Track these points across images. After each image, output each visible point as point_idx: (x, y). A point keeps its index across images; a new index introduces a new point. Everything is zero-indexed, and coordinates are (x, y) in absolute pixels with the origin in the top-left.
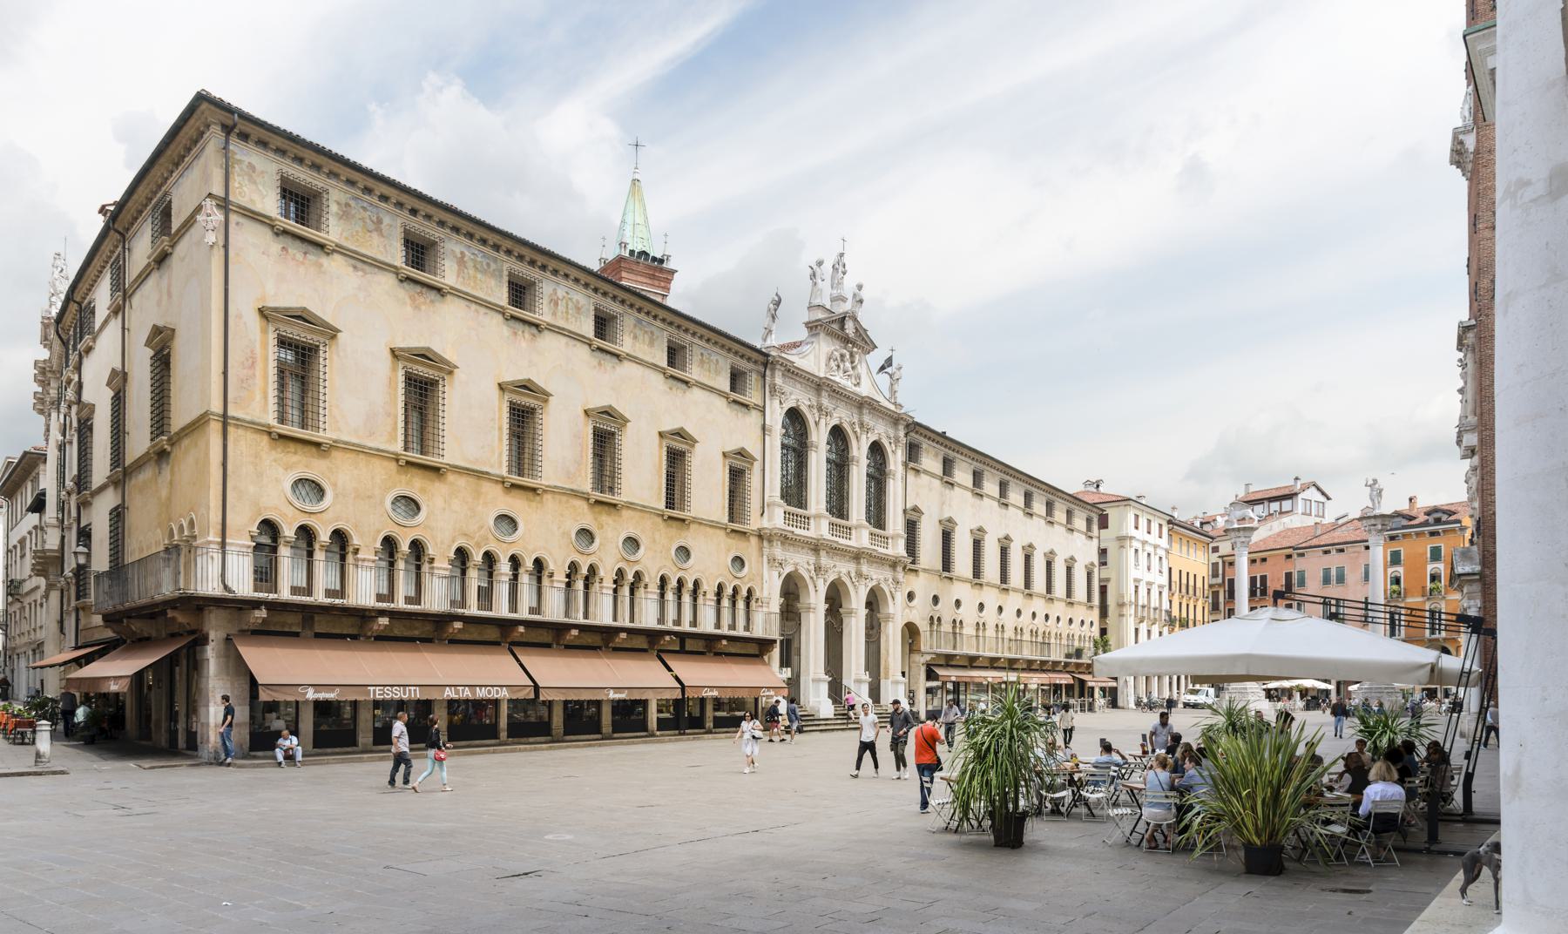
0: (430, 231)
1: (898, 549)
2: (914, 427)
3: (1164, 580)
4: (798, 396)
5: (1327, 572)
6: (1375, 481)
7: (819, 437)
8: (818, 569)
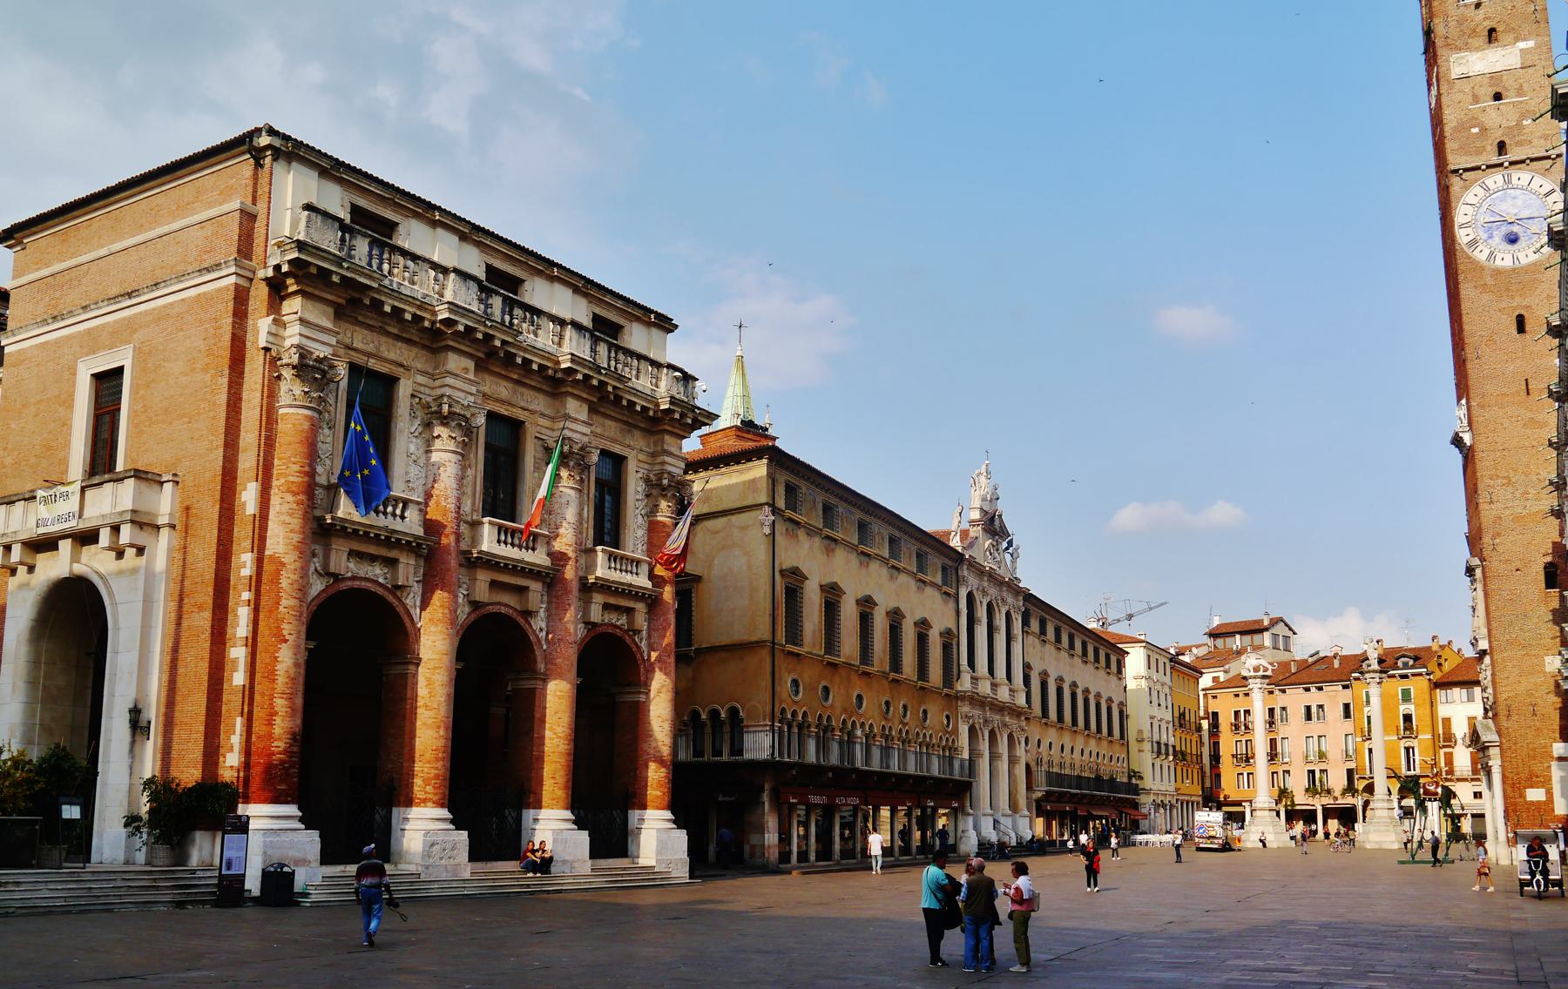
0: (833, 501)
1: (1021, 700)
2: (1030, 598)
4: (972, 581)
5: (1308, 708)
7: (982, 613)
8: (986, 721)
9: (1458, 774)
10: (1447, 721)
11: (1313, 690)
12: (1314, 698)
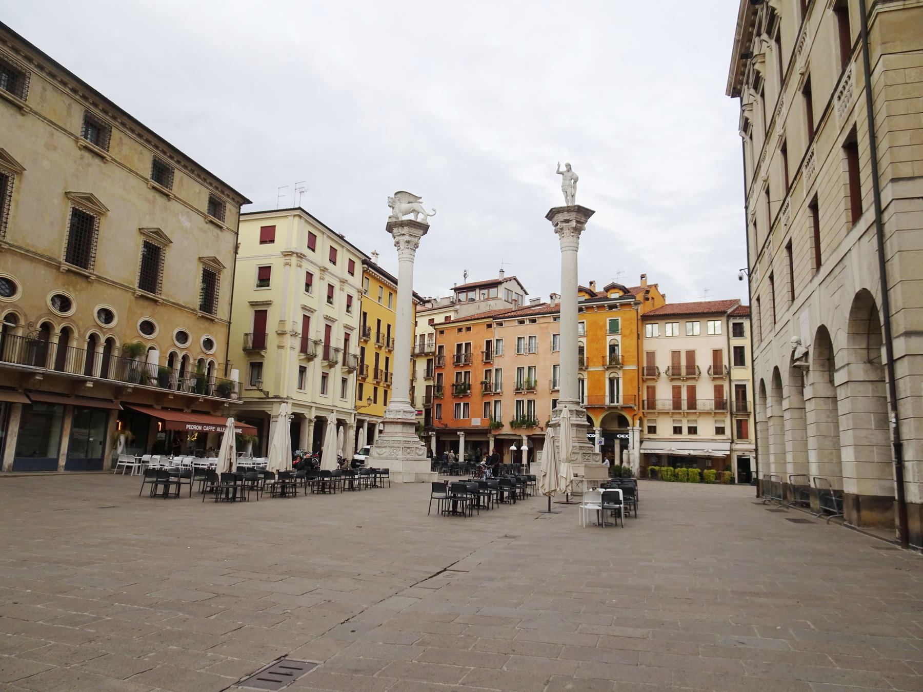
3: (354, 321)
6: (569, 167)
9: (659, 406)
10: (651, 355)
11: (527, 322)
12: (528, 329)
